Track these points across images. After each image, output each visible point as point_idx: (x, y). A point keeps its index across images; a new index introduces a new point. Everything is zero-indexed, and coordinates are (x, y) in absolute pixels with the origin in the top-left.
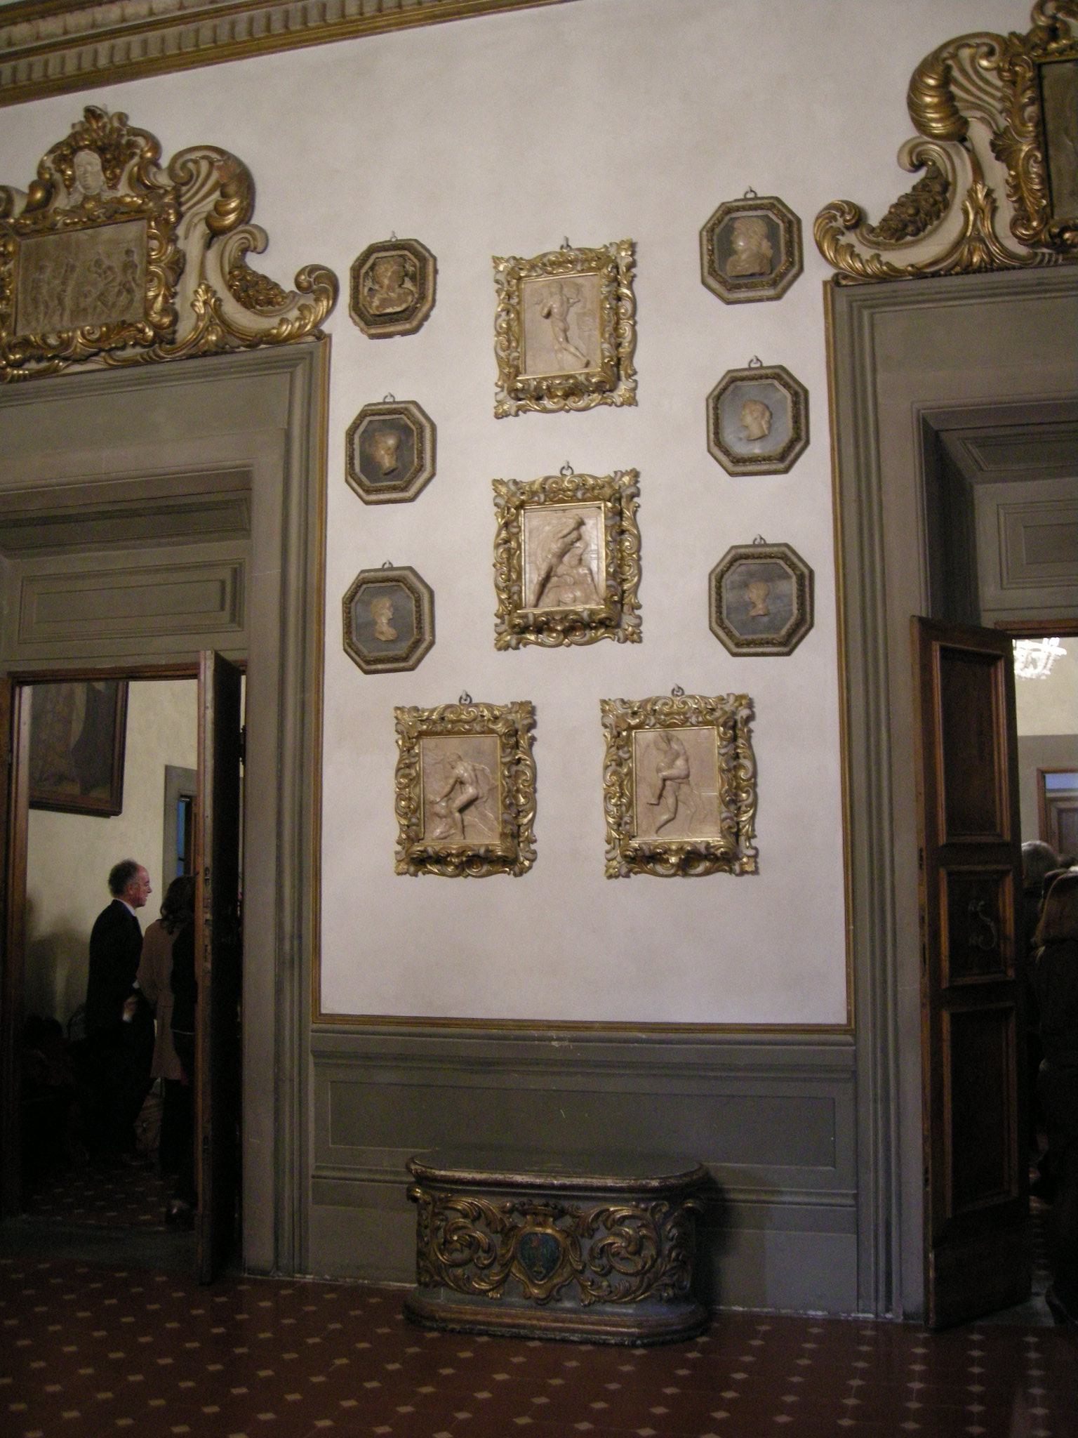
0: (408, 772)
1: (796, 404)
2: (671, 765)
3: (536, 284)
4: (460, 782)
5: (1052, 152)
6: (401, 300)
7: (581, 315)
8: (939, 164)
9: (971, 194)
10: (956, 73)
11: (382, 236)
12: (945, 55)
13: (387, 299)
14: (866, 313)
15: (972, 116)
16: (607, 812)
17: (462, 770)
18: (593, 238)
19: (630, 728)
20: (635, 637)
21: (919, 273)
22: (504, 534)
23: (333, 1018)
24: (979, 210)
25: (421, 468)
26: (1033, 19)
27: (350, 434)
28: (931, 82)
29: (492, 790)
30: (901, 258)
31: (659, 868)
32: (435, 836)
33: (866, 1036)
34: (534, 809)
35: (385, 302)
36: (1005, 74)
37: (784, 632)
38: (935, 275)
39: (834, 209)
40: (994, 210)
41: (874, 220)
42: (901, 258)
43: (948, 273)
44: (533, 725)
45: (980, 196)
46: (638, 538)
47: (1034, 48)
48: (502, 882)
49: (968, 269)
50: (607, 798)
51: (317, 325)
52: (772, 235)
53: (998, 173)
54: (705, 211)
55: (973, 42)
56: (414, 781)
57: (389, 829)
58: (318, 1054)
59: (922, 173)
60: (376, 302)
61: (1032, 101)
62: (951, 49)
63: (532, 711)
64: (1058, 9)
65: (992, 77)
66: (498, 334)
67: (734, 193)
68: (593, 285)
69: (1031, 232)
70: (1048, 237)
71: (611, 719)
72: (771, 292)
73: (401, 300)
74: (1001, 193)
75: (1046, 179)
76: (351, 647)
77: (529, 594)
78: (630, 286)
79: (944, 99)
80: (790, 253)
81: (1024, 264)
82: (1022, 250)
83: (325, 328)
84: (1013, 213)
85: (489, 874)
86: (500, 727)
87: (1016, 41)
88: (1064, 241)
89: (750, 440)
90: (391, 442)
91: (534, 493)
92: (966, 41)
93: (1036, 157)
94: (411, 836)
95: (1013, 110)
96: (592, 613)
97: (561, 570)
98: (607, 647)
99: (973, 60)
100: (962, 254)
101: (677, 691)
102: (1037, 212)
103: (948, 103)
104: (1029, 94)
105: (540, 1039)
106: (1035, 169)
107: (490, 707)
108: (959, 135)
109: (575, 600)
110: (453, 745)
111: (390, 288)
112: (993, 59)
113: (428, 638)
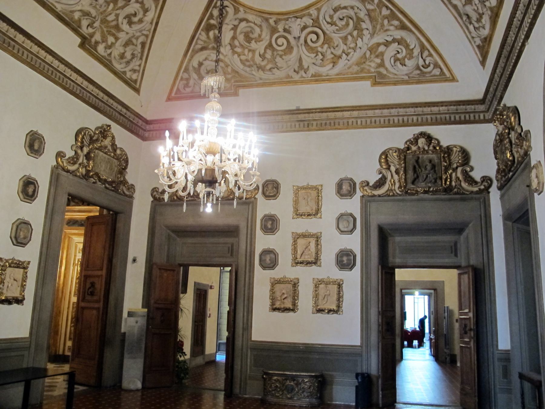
0: (272, 292)
1: (354, 221)
2: (326, 292)
3: (302, 193)
4: (283, 294)
6: (273, 192)
7: (311, 199)
8: (384, 174)
9: (391, 181)
10: (389, 155)
11: (269, 178)
13: (270, 191)
14: (368, 203)
15: (392, 164)
16: (313, 300)
17: (284, 291)
18: (313, 183)
19: (319, 284)
20: (320, 266)
21: (379, 196)
22: (294, 244)
23: (254, 341)
24: (392, 184)
25: (277, 228)
27: (262, 221)
28: (383, 157)
29: (290, 295)
30: (377, 192)
31: (323, 312)
32: (277, 305)
33: (364, 348)
34: (298, 299)
35: (270, 193)
37: (350, 266)
38: (383, 196)
39: (362, 182)
40: (395, 184)
41: (371, 184)
42: (377, 192)
43: (385, 196)
44: (298, 283)
46: (321, 246)
47: (404, 152)
48: (291, 314)
49: (389, 196)
50: (313, 298)
51: (254, 196)
52: (350, 186)
53: (396, 177)
54: (337, 180)
56: (274, 293)
57: (268, 302)
58: (251, 349)
59: (381, 175)
60: (268, 193)
61: (403, 163)
63: (298, 280)
64: (410, 143)
65: (396, 157)
66: (293, 202)
67: (343, 176)
68: (314, 193)
71: (315, 282)
72: (350, 198)
73: (273, 192)
74: (397, 181)
75: (405, 179)
76: (261, 264)
77: (298, 257)
78: (321, 194)
80: (354, 190)
81: (400, 195)
82: (400, 193)
83: (256, 196)
85: (289, 312)
86: (292, 283)
89: (344, 227)
90: (270, 222)
91: (300, 236)
94: (273, 304)
95: (400, 164)
96: (312, 261)
97: (305, 252)
98: (314, 267)
101: (328, 277)
103: (387, 161)
105: (298, 346)
106: (403, 177)
107: (290, 278)
108: (389, 168)
109: (308, 258)
110: (282, 286)
111: (271, 190)
113: (277, 264)
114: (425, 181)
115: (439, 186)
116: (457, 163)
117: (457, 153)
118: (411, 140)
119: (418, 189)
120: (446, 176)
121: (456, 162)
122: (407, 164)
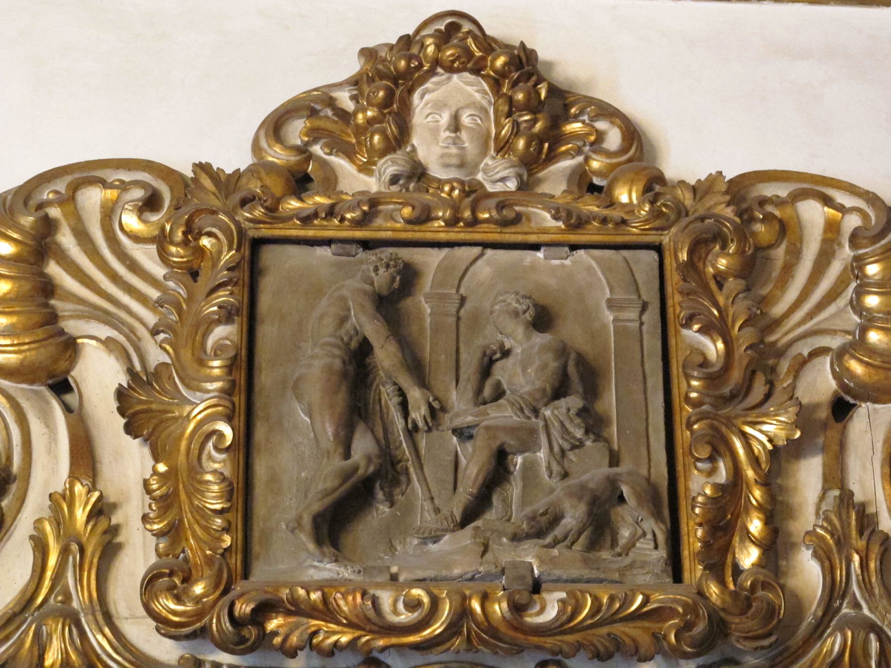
5: (260, 433)
10: (66, 239)
12: (46, 195)
26: (256, 148)
36: (173, 249)
45: (81, 515)
47: (244, 202)
55: (114, 176)
61: (227, 315)
62: (61, 186)
64: (315, 134)
69: (189, 607)
70: (227, 625)
79: (27, 286)
84: (153, 559)
87: (207, 182)
88: (264, 639)
92: (100, 173)
93: (221, 435)
99: (109, 213)
100: (21, 642)
102: (209, 561)
104: (223, 296)
112: (155, 218)
114: (470, 515)
115: (643, 578)
116: (840, 355)
117: (846, 252)
118: (331, 102)
119: (386, 598)
120: (722, 475)
121: (835, 342)
122: (267, 333)
